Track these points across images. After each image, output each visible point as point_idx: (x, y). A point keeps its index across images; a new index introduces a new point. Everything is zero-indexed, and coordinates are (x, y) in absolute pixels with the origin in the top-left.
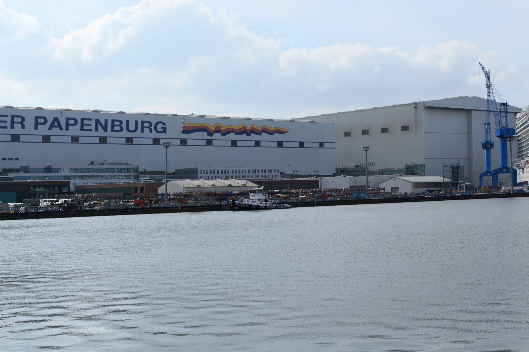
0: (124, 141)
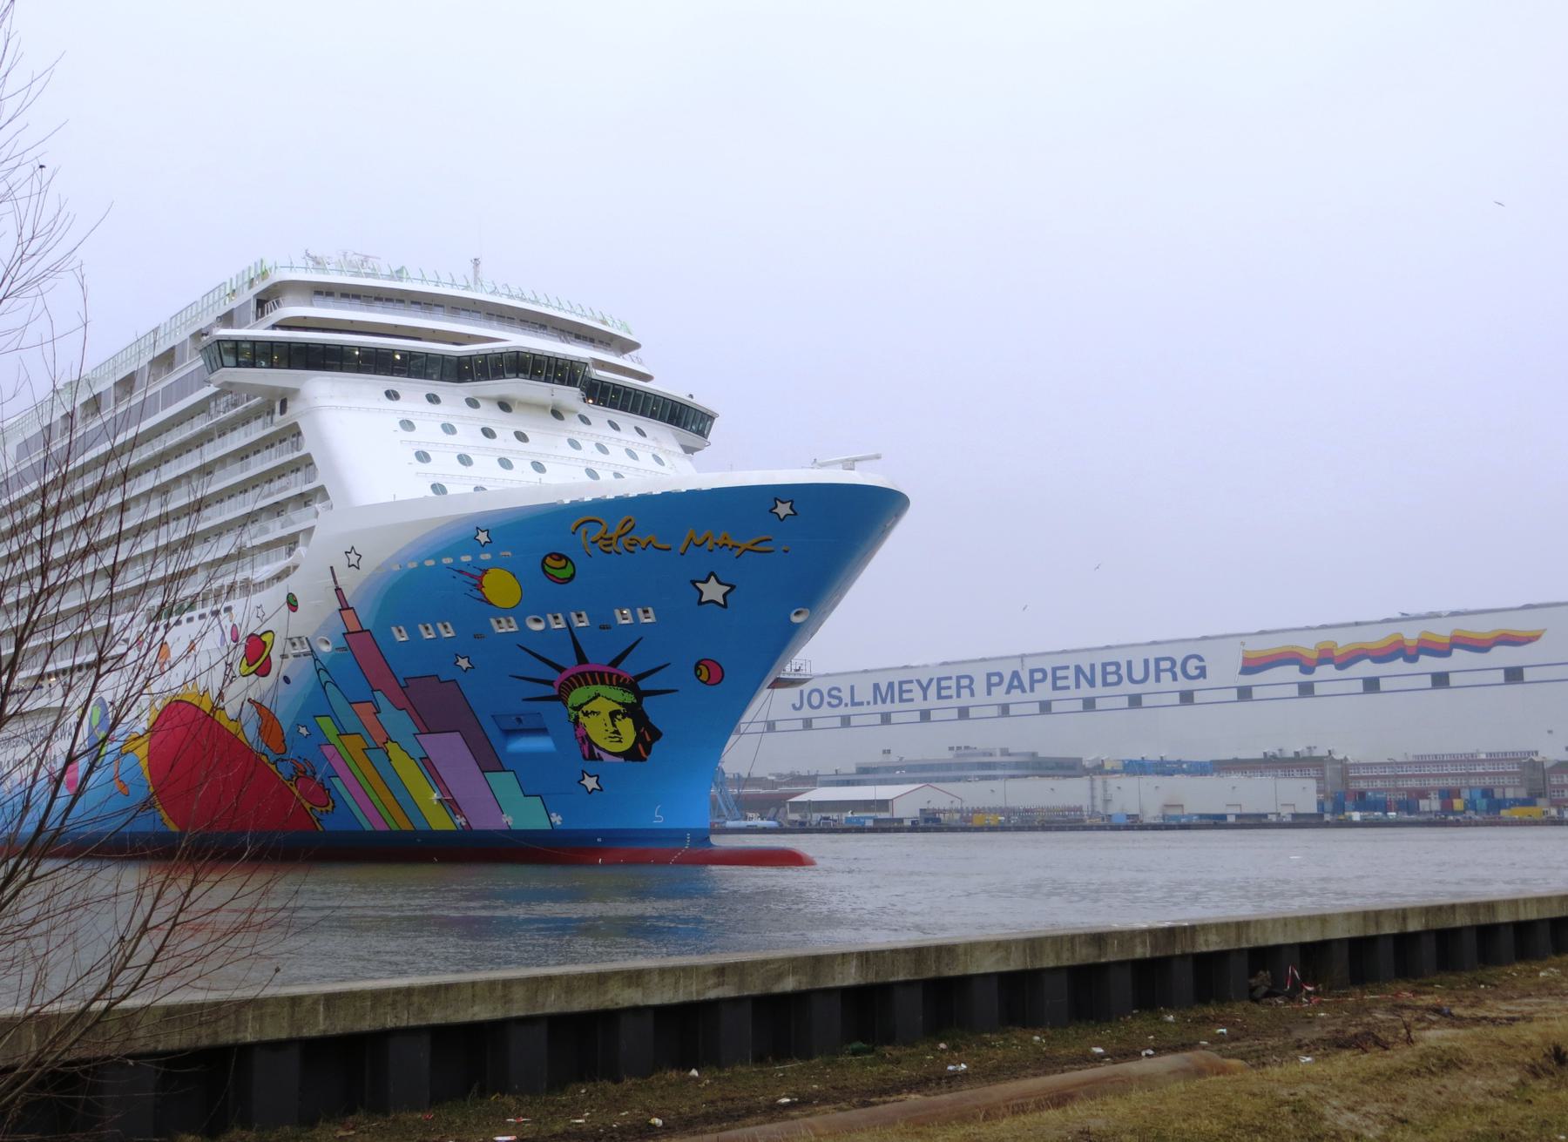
0: (1125, 702)
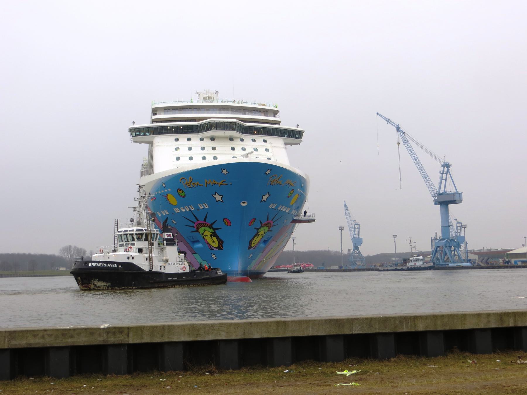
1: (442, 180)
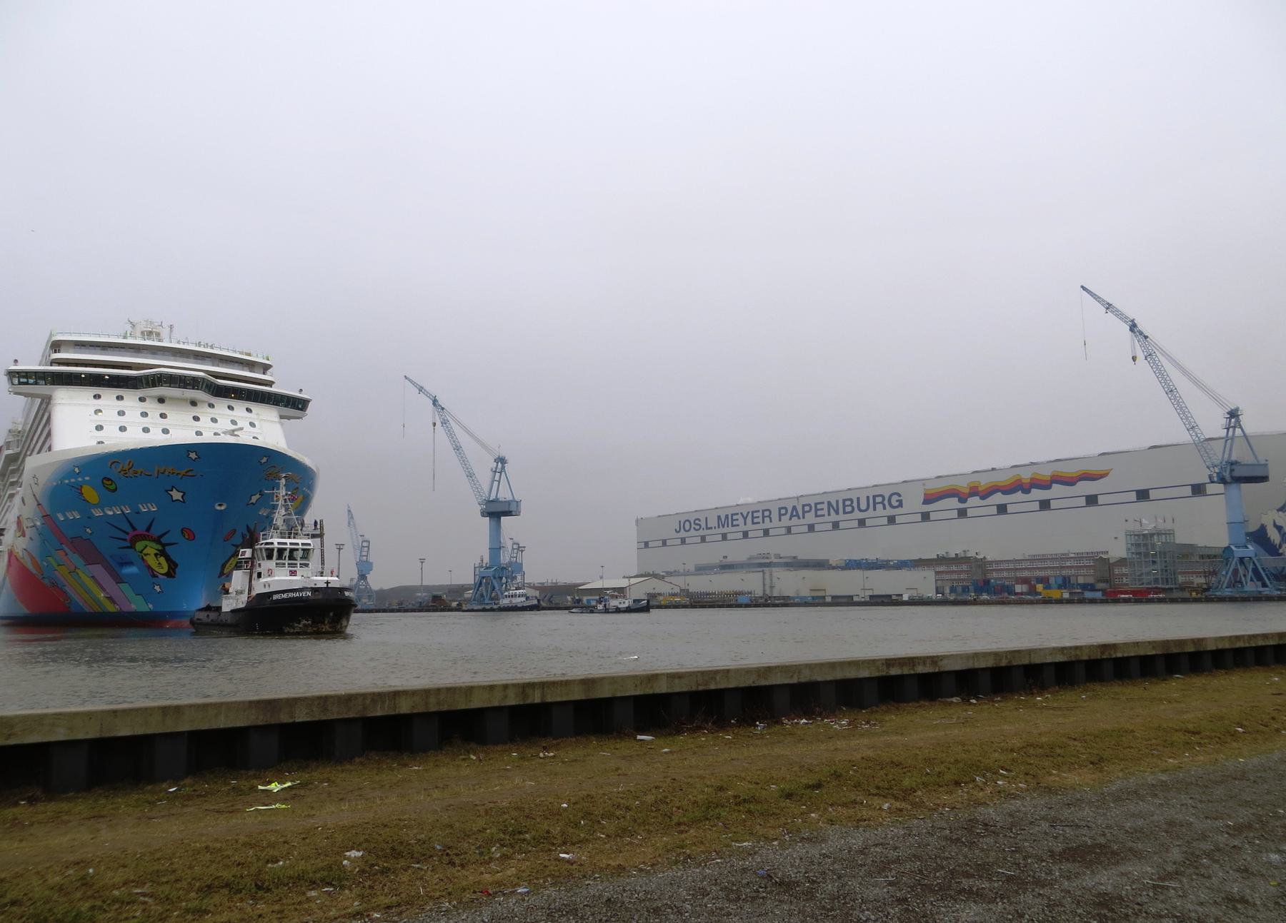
0: (856, 524)
1: (493, 481)
